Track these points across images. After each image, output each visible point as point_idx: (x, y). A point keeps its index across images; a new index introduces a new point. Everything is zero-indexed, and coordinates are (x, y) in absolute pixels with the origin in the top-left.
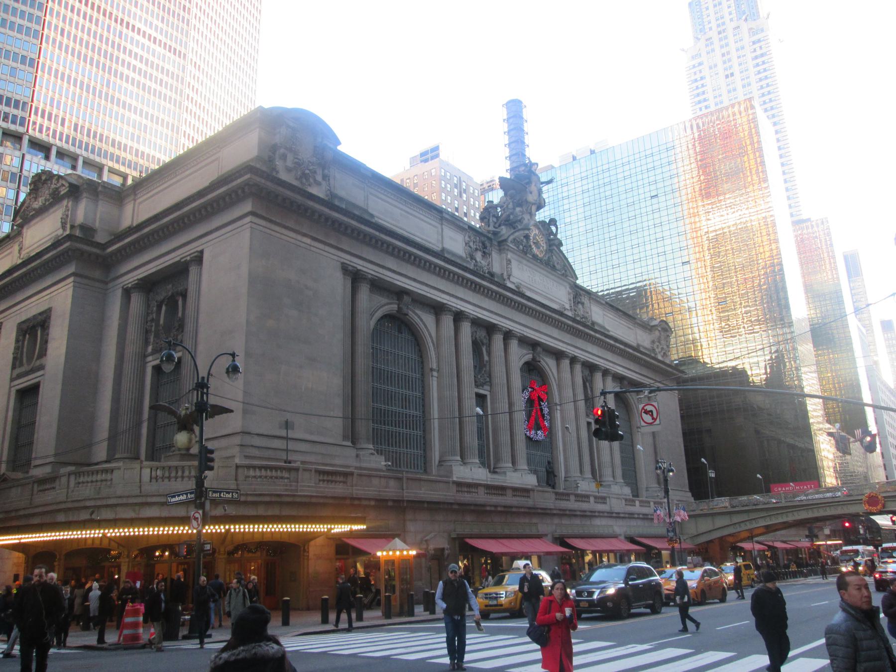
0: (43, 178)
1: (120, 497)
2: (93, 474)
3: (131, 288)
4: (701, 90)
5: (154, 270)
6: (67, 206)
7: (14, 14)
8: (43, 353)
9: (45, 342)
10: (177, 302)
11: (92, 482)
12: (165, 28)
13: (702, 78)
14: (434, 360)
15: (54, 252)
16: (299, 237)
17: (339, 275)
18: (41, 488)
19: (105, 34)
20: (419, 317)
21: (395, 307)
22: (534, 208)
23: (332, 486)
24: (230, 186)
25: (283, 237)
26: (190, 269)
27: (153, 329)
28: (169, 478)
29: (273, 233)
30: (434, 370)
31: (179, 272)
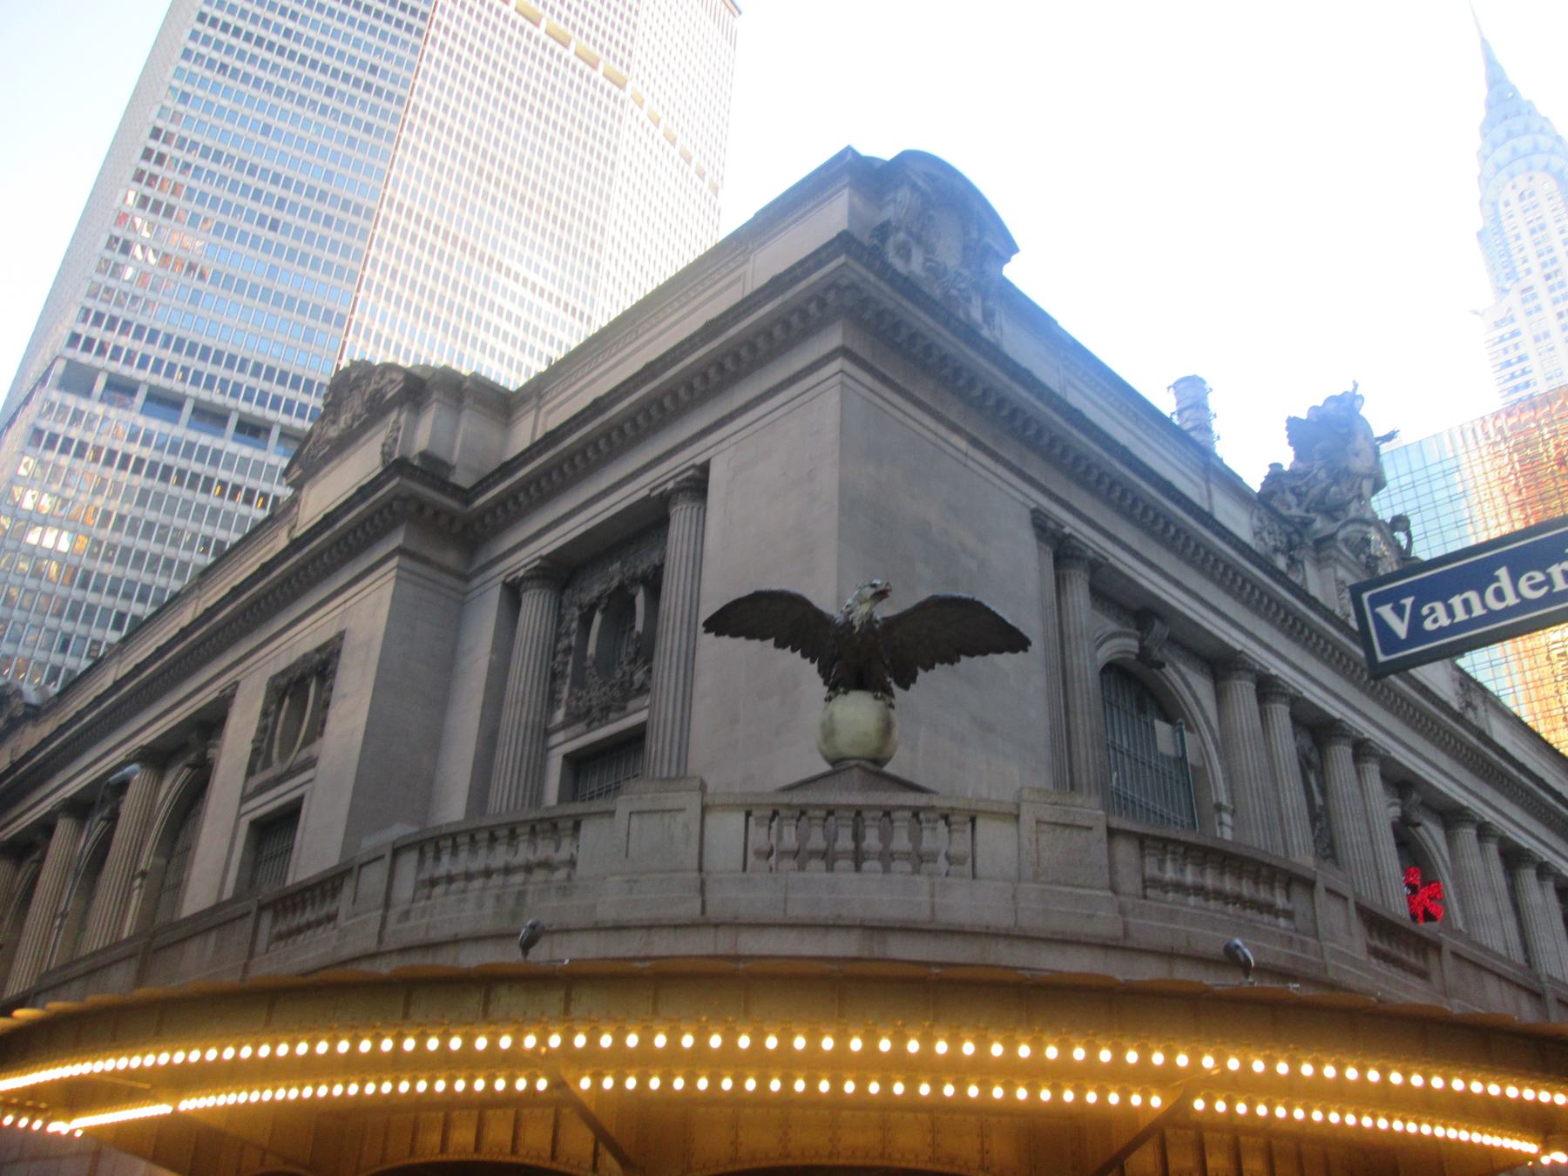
0: (353, 376)
1: (619, 928)
2: (493, 839)
3: (523, 578)
4: (1520, 380)
5: (582, 529)
6: (396, 422)
7: (321, 245)
8: (318, 729)
9: (324, 705)
10: (633, 598)
11: (488, 873)
12: (559, 273)
13: (1521, 359)
14: (1221, 785)
15: (362, 507)
16: (943, 431)
17: (1027, 535)
18: (283, 927)
19: (462, 279)
20: (1183, 678)
21: (1133, 645)
22: (1367, 486)
23: (1395, 974)
24: (789, 294)
25: (909, 421)
26: (673, 511)
27: (569, 669)
28: (828, 857)
29: (888, 407)
30: (1226, 809)
31: (647, 523)
